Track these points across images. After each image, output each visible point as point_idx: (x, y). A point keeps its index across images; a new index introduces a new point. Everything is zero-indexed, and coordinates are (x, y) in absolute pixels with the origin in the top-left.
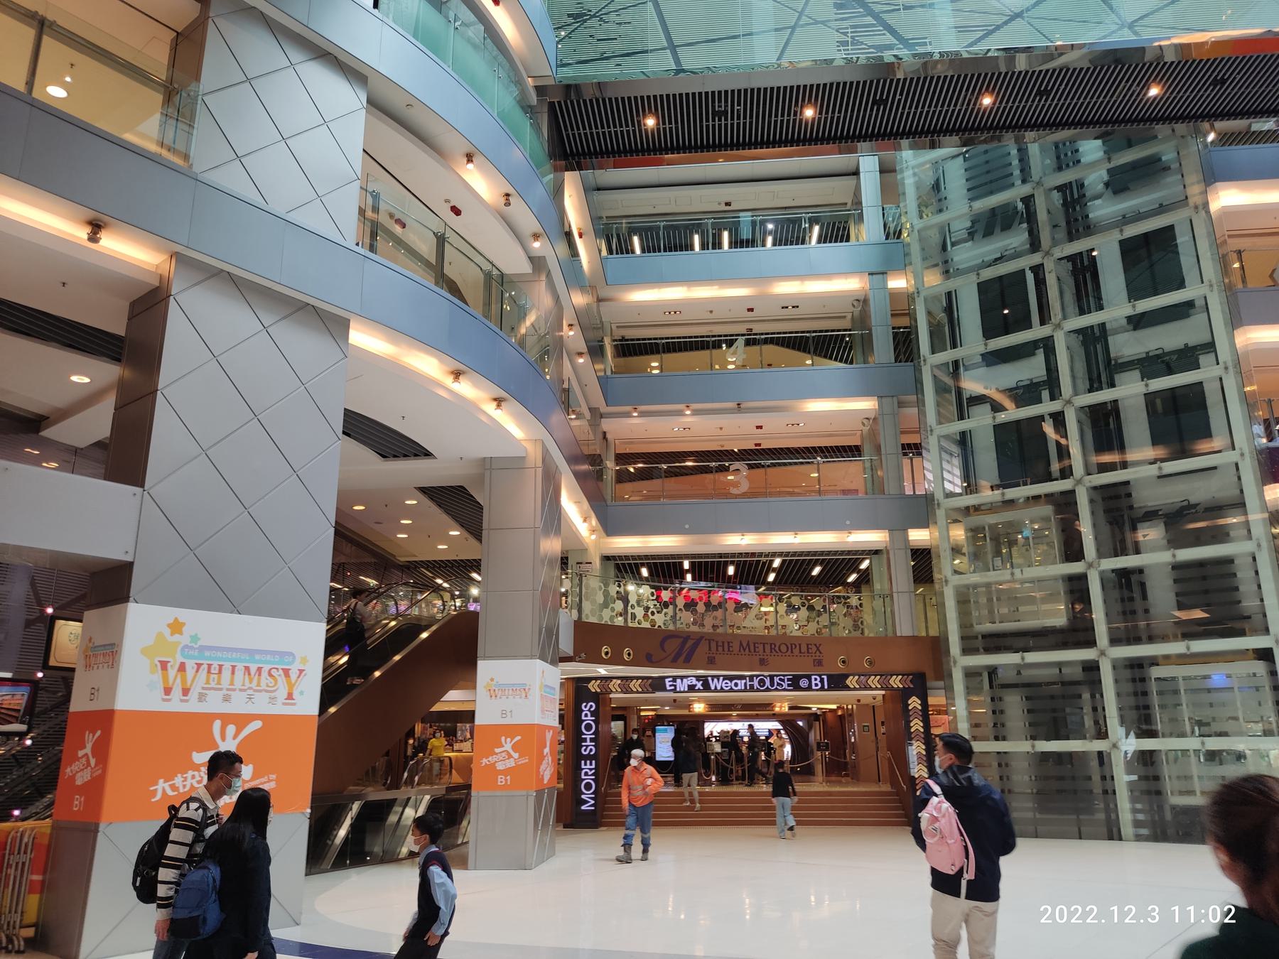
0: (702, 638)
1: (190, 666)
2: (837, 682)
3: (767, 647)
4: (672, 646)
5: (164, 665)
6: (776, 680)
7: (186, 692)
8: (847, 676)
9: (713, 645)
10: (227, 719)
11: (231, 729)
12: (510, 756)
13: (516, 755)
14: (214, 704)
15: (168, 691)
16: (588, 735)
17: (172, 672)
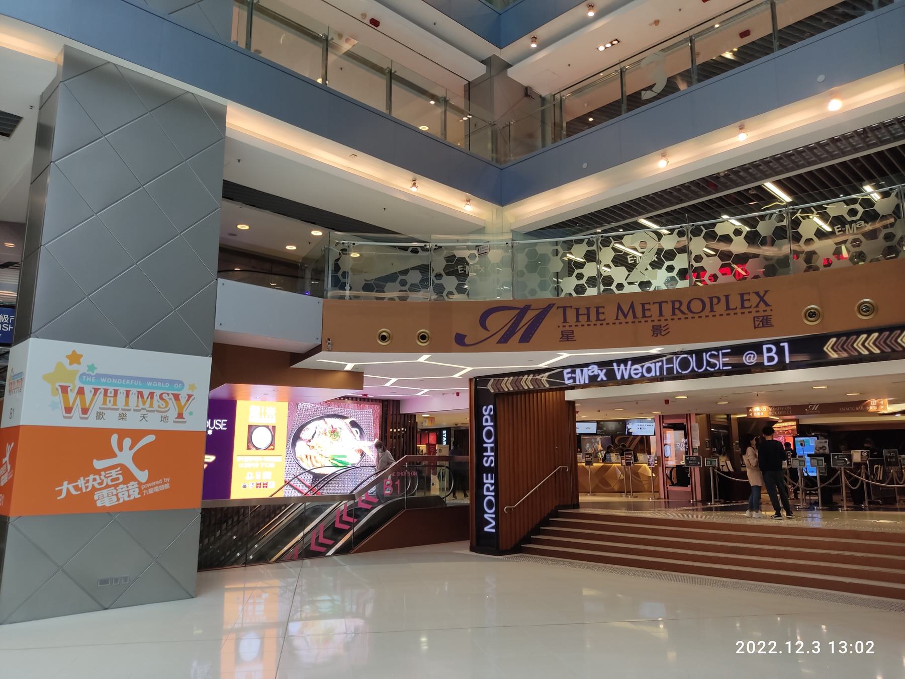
0: (550, 306)
1: (89, 390)
2: (809, 351)
3: (667, 309)
4: (498, 322)
5: (64, 389)
6: (706, 357)
7: (85, 411)
8: (825, 338)
9: (571, 315)
10: (123, 434)
11: (127, 442)
12: (128, 477)
13: (142, 476)
14: (111, 421)
15: (68, 410)
16: (489, 444)
17: (72, 395)
